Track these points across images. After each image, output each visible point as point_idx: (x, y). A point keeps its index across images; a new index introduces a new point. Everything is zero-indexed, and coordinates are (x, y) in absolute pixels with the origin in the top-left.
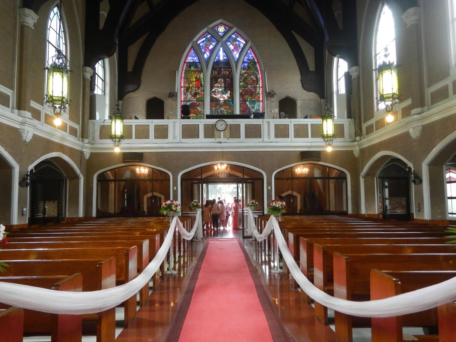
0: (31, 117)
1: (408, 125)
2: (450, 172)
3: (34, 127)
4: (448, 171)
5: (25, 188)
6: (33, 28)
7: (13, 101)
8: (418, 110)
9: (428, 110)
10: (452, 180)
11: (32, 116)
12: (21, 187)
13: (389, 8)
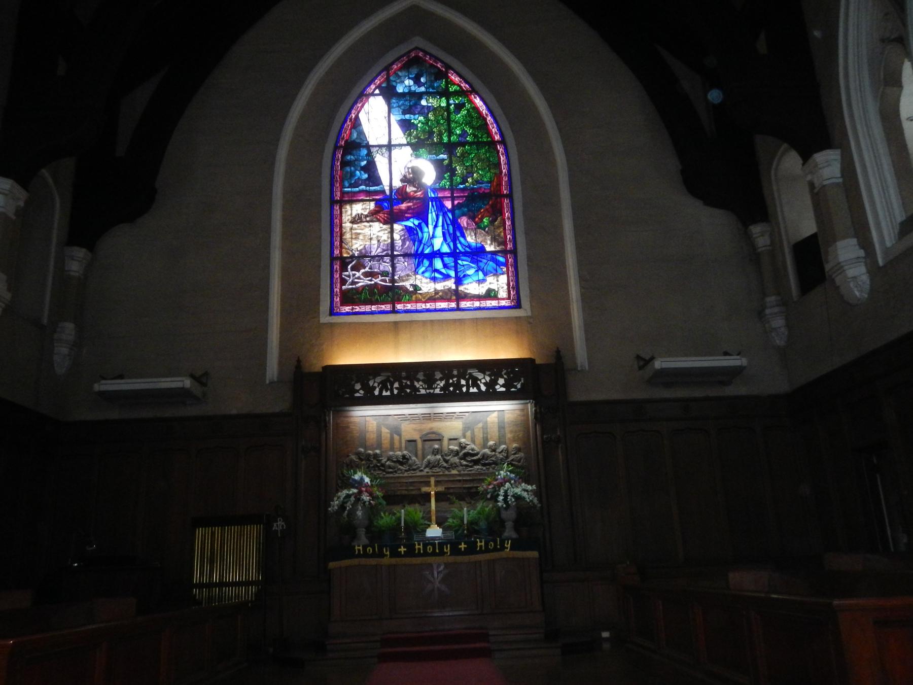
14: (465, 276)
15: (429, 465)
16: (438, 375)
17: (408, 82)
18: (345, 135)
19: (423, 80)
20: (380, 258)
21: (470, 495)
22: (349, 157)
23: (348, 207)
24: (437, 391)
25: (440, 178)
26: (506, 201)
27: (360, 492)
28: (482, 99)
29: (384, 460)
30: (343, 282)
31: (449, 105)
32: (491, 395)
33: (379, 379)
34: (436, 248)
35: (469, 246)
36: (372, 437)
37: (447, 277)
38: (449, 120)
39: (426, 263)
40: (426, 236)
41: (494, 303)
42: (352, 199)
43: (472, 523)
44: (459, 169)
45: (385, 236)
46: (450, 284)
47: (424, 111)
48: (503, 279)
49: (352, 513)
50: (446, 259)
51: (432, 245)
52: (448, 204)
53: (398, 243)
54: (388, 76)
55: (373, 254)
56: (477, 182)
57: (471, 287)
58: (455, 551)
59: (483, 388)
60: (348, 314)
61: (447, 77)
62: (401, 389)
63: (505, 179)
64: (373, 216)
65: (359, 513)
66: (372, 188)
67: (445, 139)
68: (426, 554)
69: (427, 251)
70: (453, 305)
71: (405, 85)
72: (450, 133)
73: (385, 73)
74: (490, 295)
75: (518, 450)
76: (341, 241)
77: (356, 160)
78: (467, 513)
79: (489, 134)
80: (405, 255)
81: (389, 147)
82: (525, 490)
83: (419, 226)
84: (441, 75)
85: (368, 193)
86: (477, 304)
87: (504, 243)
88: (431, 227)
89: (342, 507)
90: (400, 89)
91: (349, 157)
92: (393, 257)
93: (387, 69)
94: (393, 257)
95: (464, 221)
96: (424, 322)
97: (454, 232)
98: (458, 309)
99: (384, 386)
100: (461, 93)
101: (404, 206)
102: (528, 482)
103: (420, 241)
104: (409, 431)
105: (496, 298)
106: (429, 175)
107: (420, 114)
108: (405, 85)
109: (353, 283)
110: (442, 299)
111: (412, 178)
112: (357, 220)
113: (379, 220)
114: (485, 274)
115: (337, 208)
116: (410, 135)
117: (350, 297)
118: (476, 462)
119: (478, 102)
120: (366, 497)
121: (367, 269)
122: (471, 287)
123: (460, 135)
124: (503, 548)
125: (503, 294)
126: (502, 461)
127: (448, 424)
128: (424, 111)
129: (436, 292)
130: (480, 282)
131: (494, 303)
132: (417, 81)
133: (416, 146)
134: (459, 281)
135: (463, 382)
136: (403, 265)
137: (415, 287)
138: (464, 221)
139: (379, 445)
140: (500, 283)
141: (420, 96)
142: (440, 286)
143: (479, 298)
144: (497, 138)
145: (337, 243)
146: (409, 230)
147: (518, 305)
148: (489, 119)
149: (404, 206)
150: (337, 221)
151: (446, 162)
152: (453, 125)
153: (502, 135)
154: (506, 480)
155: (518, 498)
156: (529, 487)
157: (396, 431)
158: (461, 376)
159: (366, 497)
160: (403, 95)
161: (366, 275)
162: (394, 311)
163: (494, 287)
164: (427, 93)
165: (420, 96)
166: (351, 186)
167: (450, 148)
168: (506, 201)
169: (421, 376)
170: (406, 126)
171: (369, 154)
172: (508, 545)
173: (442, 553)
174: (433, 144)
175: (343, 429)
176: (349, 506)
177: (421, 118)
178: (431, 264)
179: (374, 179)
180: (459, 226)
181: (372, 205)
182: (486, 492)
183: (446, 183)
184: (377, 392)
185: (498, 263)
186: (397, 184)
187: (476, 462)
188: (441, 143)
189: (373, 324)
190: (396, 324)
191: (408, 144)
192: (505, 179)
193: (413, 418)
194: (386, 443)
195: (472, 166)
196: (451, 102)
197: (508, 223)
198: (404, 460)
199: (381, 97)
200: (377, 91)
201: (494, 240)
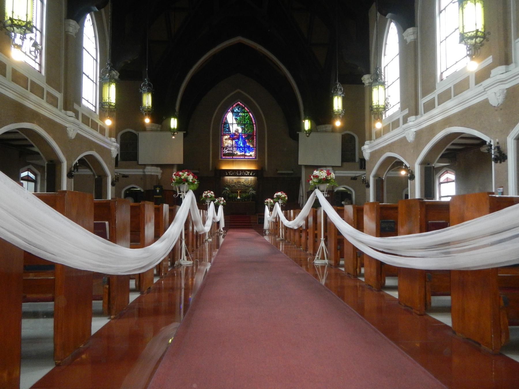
0: (75, 117)
1: (405, 130)
2: (447, 173)
3: (78, 126)
4: (446, 172)
5: (71, 179)
6: (75, 37)
7: (60, 103)
8: (412, 118)
9: (421, 117)
10: (449, 180)
11: (75, 116)
12: (68, 178)
13: (395, 25)
14: (246, 152)
15: (238, 187)
16: (241, 172)
17: (237, 109)
18: (224, 121)
19: (240, 109)
20: (230, 147)
21: (245, 192)
22: (225, 126)
23: (224, 137)
24: (240, 174)
25: (242, 131)
26: (255, 137)
27: (227, 191)
28: (251, 114)
29: (230, 186)
30: (223, 152)
31: (245, 115)
32: (249, 176)
33: (230, 172)
34: (241, 146)
35: (247, 146)
36: (228, 182)
37: (243, 152)
38: (244, 118)
39: (239, 149)
40: (239, 143)
41: (251, 157)
42: (225, 135)
43: (245, 197)
44: (246, 129)
45: (231, 143)
46: (243, 153)
47: (240, 116)
48: (253, 153)
49: (226, 194)
50: (243, 148)
51: (240, 145)
52: (244, 137)
53: (234, 144)
54: (233, 107)
55: (229, 146)
56: (249, 132)
57: (247, 154)
58: (242, 200)
59: (248, 174)
60: (224, 158)
61: (245, 109)
62: (234, 174)
63: (255, 132)
64: (229, 139)
65: (227, 194)
66: (230, 133)
67: (244, 123)
68: (237, 201)
69: (239, 146)
70: (244, 157)
71: (236, 110)
72: (245, 121)
73: (232, 107)
74: (251, 156)
75: (254, 185)
76: (223, 144)
77: (226, 126)
78: (244, 195)
79: (252, 122)
80: (235, 147)
81: (233, 124)
82: (254, 192)
83: (238, 141)
84: (243, 108)
85: (228, 134)
86: (248, 157)
87: (254, 145)
88: (240, 141)
89: (224, 193)
90: (235, 111)
91: (225, 126)
92: (233, 147)
93: (233, 106)
94: (233, 147)
95: (247, 141)
96: (238, 161)
97: (244, 143)
98: (245, 158)
99: (231, 173)
100: (247, 112)
101: (235, 137)
102: (255, 191)
103: (238, 144)
104: (235, 181)
105: (252, 156)
106: (240, 131)
107: (239, 117)
108: (236, 110)
109: (225, 152)
110: (242, 156)
111: (237, 131)
112: (226, 139)
113: (230, 140)
114: (250, 152)
115: (222, 137)
116: (237, 121)
117: (224, 155)
118: (246, 187)
119: (251, 115)
120: (228, 192)
121: (228, 149)
122: (247, 154)
123: (247, 122)
124: (250, 201)
125: (253, 156)
126: (251, 187)
127: (242, 180)
128: (240, 116)
129: (241, 154)
130: (249, 153)
131: (251, 157)
132: (238, 109)
133: (238, 124)
134: (245, 152)
135: (245, 173)
136: (235, 149)
137: (237, 154)
138: (247, 141)
139: (230, 183)
140: (252, 153)
141: (239, 113)
142: (242, 153)
143: (249, 156)
144: (254, 123)
145: (222, 144)
146: (236, 142)
147: (256, 158)
148: (253, 119)
149: (235, 137)
150: (222, 139)
151: (244, 128)
152: (245, 120)
153: (255, 122)
154: (251, 190)
155: (253, 193)
156: (255, 192)
157: (233, 181)
158: (244, 172)
159: (228, 192)
160: (236, 112)
161: (228, 151)
162: (233, 158)
163: (252, 154)
164: (240, 112)
165: (239, 113)
166: (225, 132)
167: (244, 125)
168: (255, 137)
169: (237, 172)
170: (236, 119)
171: (229, 125)
172: (251, 200)
173: (240, 201)
174: (241, 124)
175: (224, 181)
176: (225, 194)
177: (239, 118)
178: (240, 149)
179: (229, 131)
180: (246, 141)
181: (229, 136)
182: (247, 192)
183: (244, 132)
184: (230, 174)
185: (252, 149)
186: (234, 132)
187: (246, 187)
188: (243, 124)
189: (229, 161)
190: (233, 161)
191: (237, 123)
192: (255, 132)
193: (234, 178)
194: (231, 182)
195: (249, 129)
196: (245, 114)
197: (255, 141)
198: (234, 186)
199: (231, 113)
200: (230, 111)
201: (252, 145)
